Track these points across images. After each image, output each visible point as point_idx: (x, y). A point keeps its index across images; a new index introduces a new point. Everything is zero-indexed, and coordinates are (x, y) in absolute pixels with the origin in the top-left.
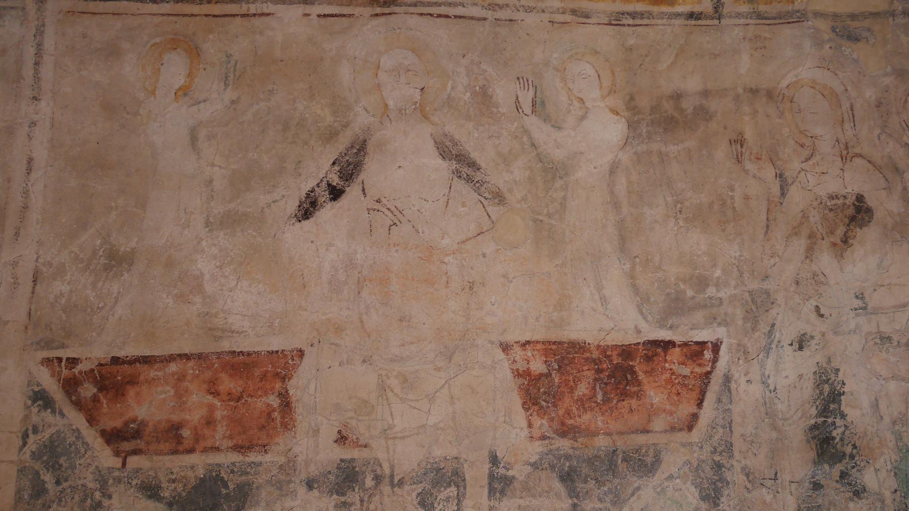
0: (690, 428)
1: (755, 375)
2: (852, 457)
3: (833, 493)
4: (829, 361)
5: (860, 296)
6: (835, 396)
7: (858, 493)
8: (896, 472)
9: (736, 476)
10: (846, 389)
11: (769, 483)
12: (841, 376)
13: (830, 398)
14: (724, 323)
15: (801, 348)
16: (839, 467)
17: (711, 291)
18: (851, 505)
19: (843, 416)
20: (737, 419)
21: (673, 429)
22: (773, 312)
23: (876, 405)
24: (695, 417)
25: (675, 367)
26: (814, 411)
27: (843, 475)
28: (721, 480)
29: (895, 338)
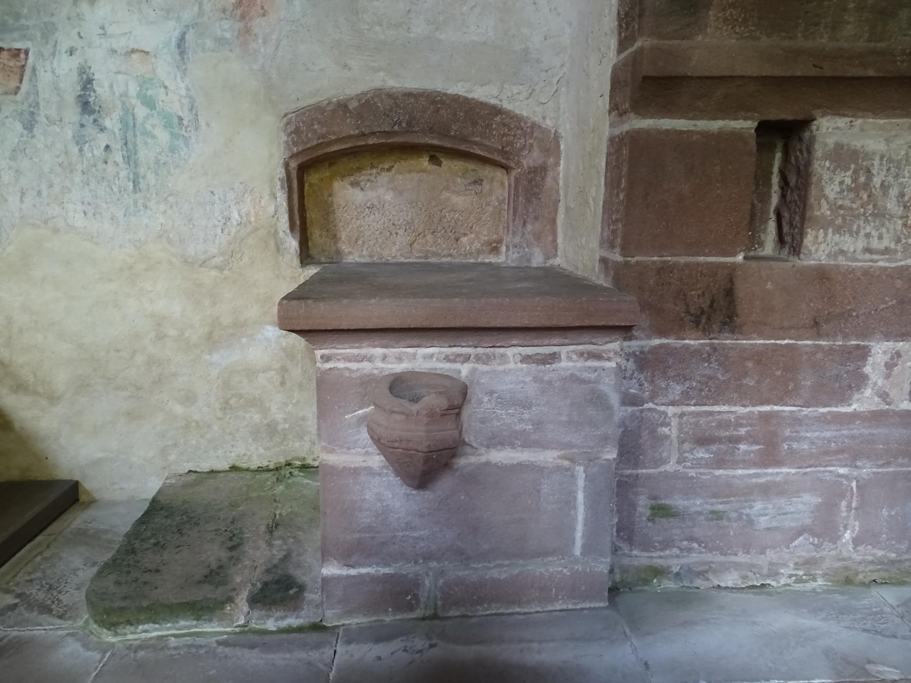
0: (16, 93)
1: (48, 67)
2: (99, 112)
3: (91, 130)
4: (86, 62)
5: (102, 28)
6: (90, 81)
7: (102, 130)
8: (122, 120)
9: (41, 118)
10: (95, 77)
11: (58, 123)
12: (92, 71)
13: (87, 83)
14: (30, 39)
15: (71, 55)
16: (92, 117)
17: (23, 21)
18: (99, 135)
19: (95, 91)
20: (40, 90)
21: (6, 93)
22: (57, 34)
23: (111, 87)
24: (18, 88)
25: (5, 62)
26: (79, 88)
27: (95, 121)
28: (34, 120)
29: (119, 51)
